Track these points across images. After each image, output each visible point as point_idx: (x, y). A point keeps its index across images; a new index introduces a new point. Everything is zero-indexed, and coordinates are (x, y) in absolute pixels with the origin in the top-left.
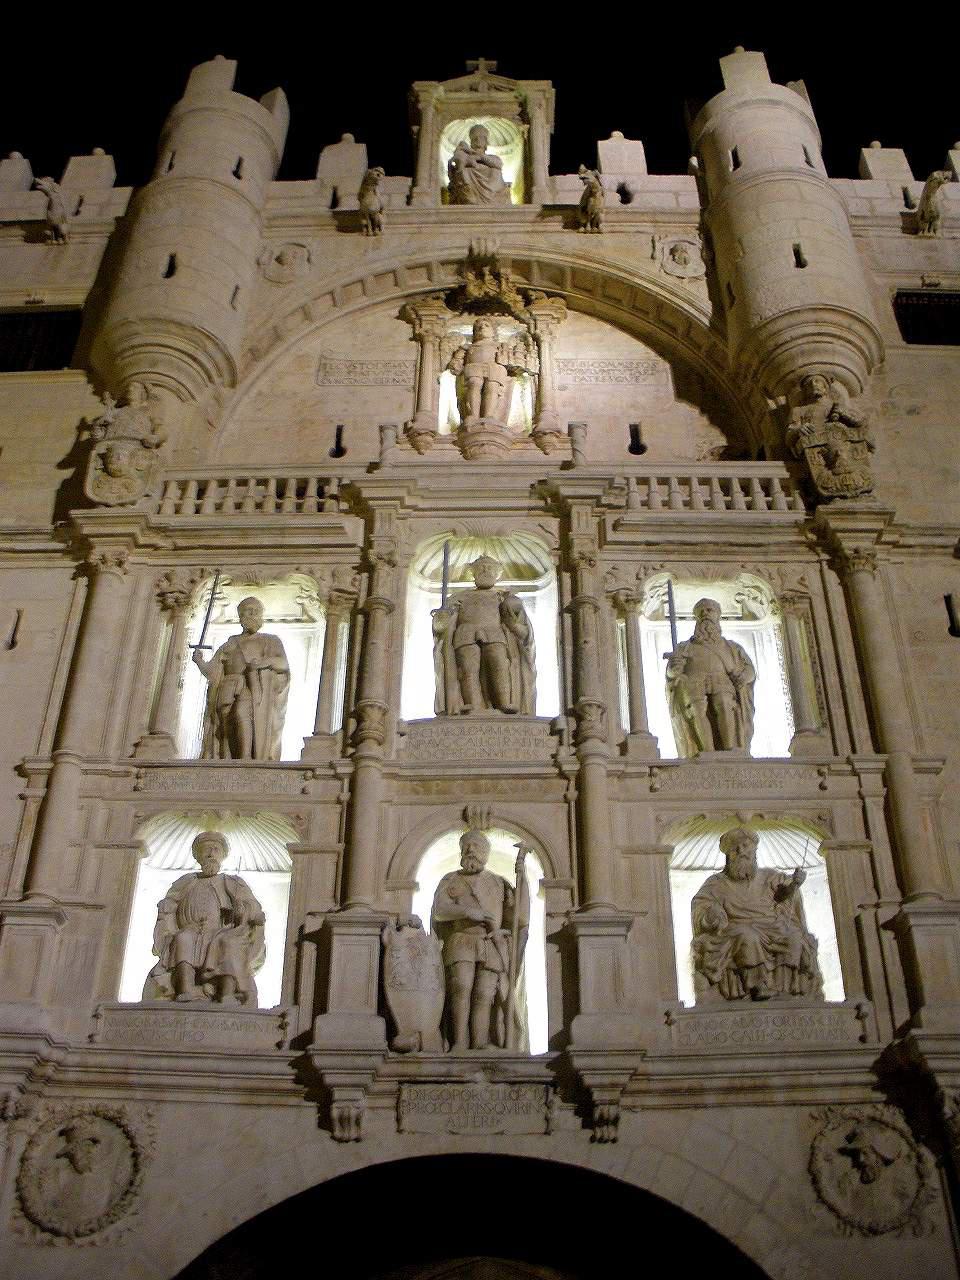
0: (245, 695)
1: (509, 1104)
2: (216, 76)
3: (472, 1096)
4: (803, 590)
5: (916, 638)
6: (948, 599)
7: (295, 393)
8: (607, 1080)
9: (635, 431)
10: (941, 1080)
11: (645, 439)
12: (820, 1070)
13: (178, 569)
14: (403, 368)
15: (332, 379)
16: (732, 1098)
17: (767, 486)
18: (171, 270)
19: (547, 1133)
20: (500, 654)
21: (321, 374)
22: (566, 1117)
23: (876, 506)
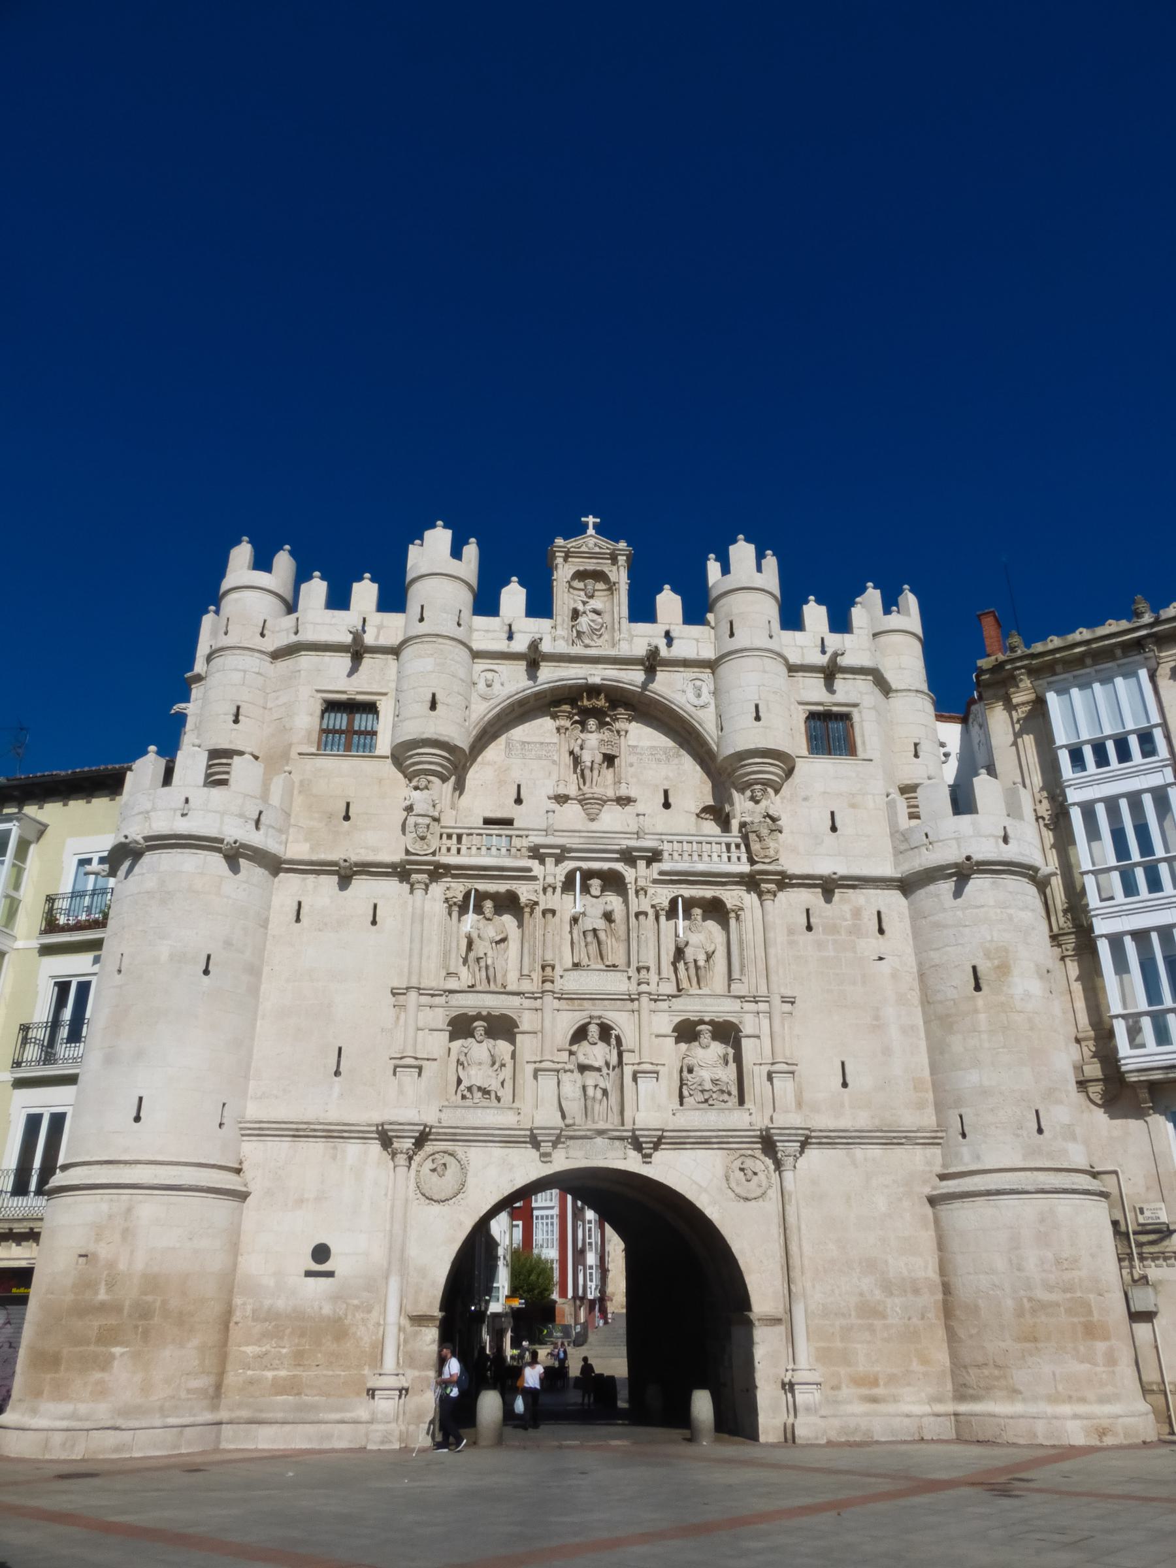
0: (490, 954)
1: (610, 1147)
2: (439, 538)
3: (595, 1143)
4: (740, 905)
5: (791, 932)
6: (808, 911)
8: (648, 1140)
9: (666, 792)
10: (778, 1144)
11: (671, 800)
12: (732, 1137)
13: (452, 884)
15: (513, 753)
16: (697, 1146)
17: (728, 846)
18: (433, 706)
19: (625, 1159)
20: (602, 935)
21: (508, 750)
22: (633, 1154)
23: (779, 868)
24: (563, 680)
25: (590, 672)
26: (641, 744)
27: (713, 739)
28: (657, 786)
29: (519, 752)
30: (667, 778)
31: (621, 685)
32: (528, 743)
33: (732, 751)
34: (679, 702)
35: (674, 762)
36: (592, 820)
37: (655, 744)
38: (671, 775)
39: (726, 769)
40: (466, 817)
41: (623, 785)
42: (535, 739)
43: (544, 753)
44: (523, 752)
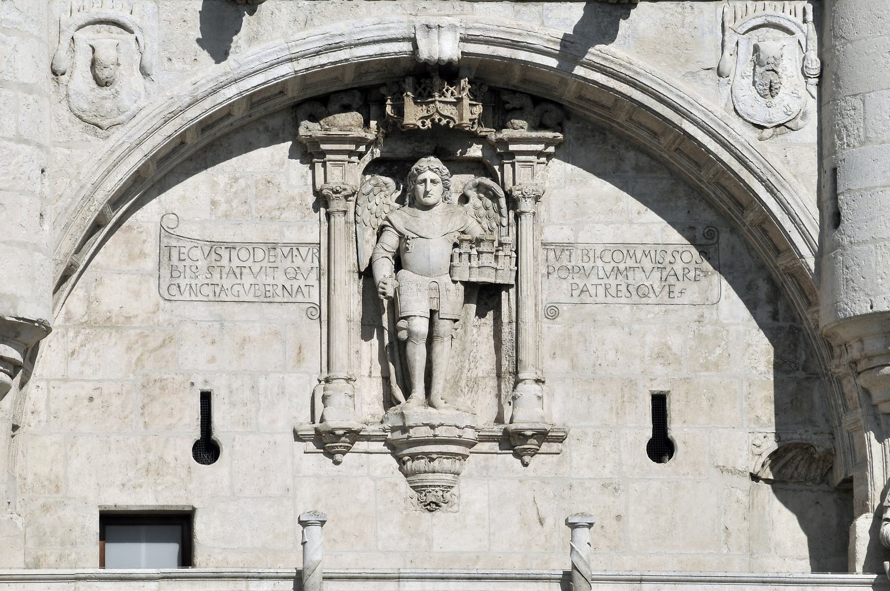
7: (128, 318)
9: (659, 402)
11: (675, 431)
14: (298, 261)
15: (183, 282)
21: (165, 272)
24: (338, 47)
25: (423, 20)
26: (583, 237)
27: (804, 234)
28: (631, 383)
29: (202, 279)
30: (662, 355)
31: (523, 55)
32: (231, 247)
33: (864, 308)
34: (707, 111)
35: (686, 299)
36: (432, 506)
37: (631, 235)
38: (675, 341)
39: (846, 345)
40: (45, 508)
41: (527, 390)
42: (251, 233)
43: (281, 280)
44: (216, 279)
